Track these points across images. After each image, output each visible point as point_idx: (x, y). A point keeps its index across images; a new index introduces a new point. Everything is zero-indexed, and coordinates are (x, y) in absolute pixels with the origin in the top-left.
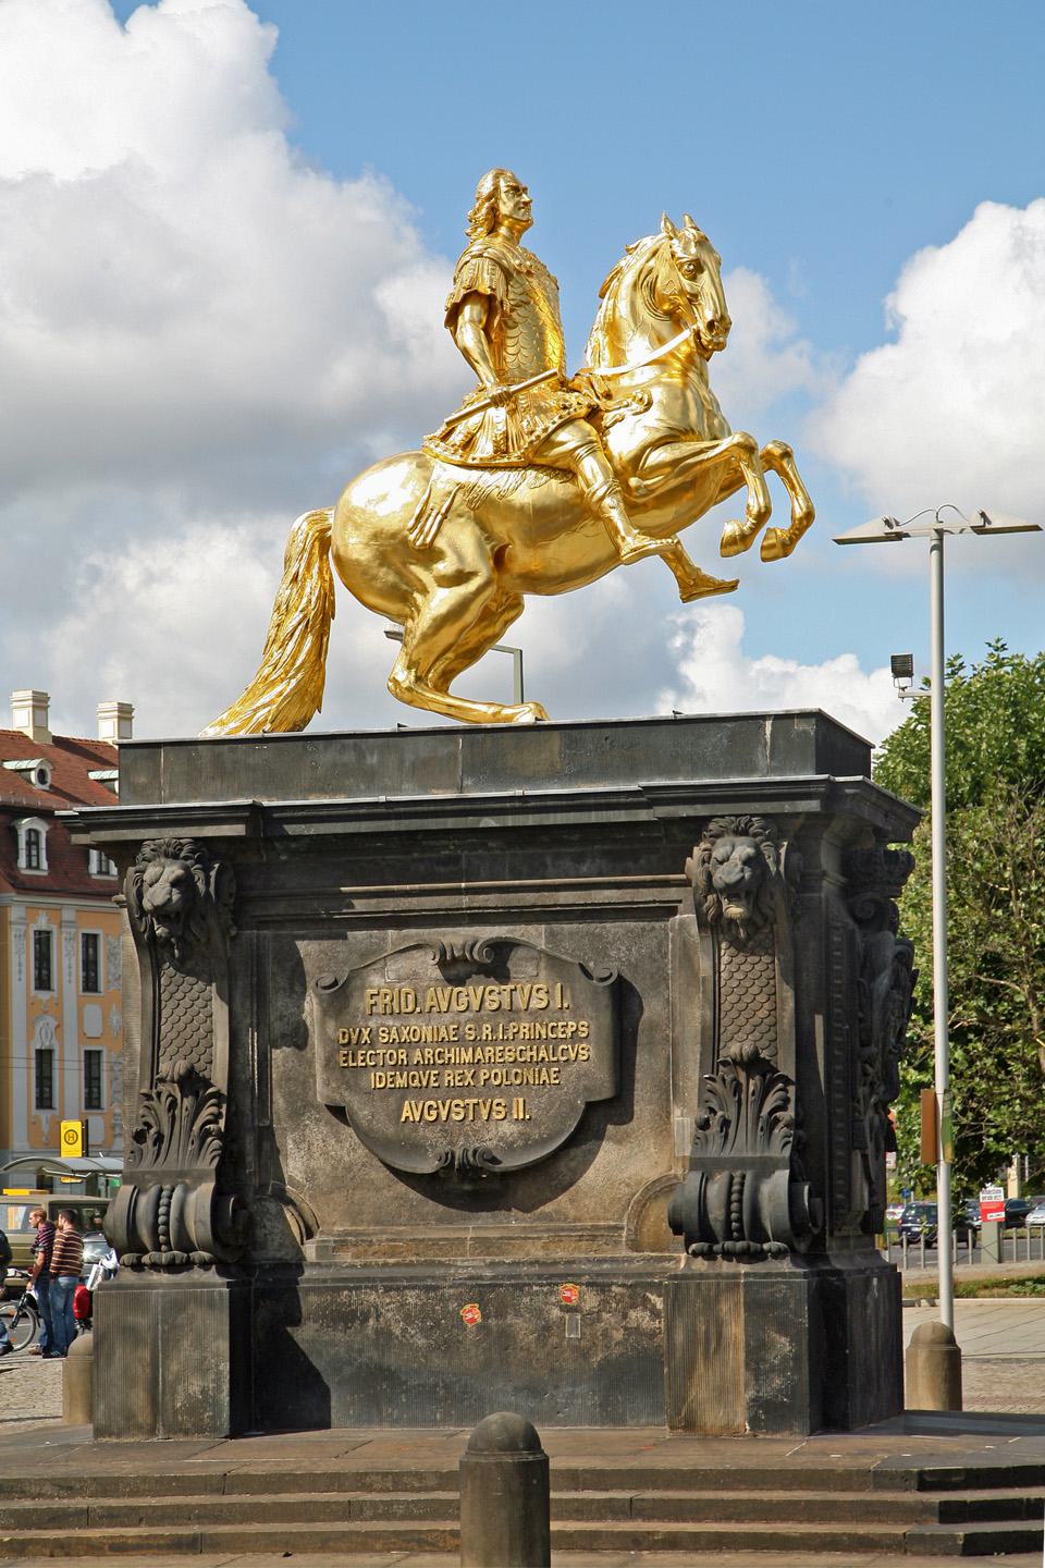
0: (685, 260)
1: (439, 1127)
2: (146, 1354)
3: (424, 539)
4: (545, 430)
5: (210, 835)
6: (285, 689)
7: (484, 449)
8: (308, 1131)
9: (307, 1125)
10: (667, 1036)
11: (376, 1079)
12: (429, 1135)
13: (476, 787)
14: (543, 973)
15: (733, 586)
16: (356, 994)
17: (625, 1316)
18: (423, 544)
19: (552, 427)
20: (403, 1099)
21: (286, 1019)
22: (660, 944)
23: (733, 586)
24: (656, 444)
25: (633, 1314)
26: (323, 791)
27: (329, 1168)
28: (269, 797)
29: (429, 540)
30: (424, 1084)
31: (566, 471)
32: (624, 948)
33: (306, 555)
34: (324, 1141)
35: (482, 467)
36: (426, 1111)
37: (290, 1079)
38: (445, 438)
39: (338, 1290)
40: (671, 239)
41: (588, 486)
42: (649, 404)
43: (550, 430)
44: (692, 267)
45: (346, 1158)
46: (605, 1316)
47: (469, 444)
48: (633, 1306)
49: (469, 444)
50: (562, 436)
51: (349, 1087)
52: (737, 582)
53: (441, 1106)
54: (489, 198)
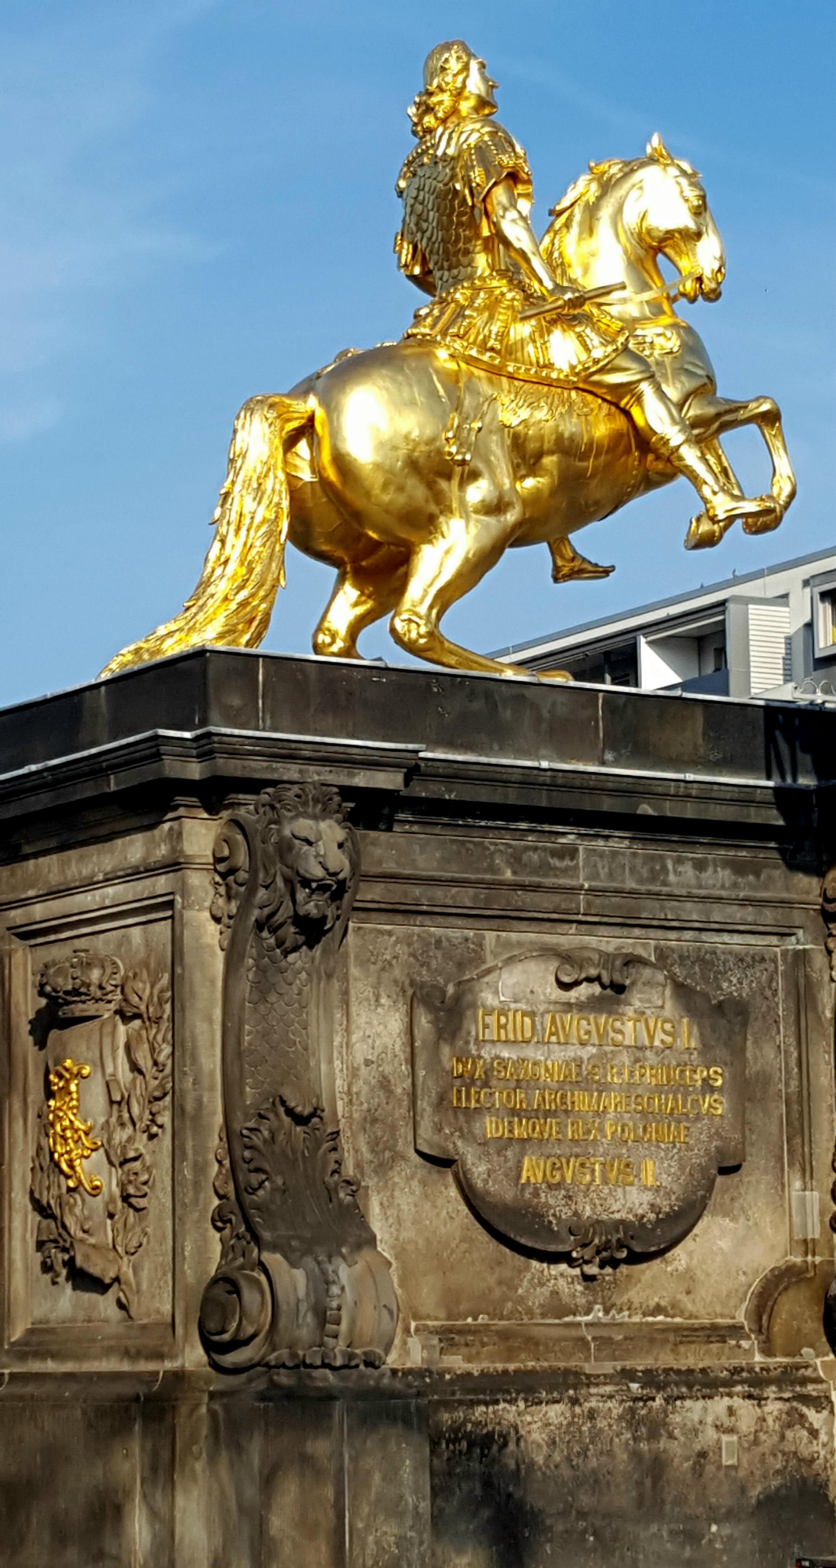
1: (563, 1192)
2: (329, 1492)
5: (362, 784)
8: (397, 1193)
9: (395, 1184)
10: (780, 1090)
11: (490, 1127)
12: (552, 1201)
13: (616, 763)
14: (669, 1005)
16: (469, 1013)
17: (783, 1437)
20: (523, 1154)
21: (370, 1041)
22: (771, 979)
25: (789, 1434)
26: (451, 745)
27: (421, 1242)
28: (434, 744)
30: (546, 1136)
32: (735, 980)
34: (416, 1206)
36: (548, 1173)
37: (375, 1120)
39: (473, 1404)
45: (443, 1230)
46: (763, 1437)
48: (790, 1425)
51: (462, 1136)
53: (565, 1165)
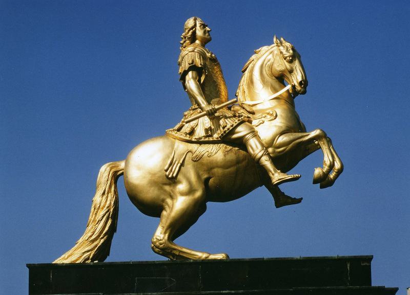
0: (288, 55)
3: (173, 174)
4: (232, 126)
6: (98, 244)
7: (200, 133)
15: (299, 201)
18: (172, 177)
19: (235, 125)
23: (299, 201)
24: (282, 133)
29: (174, 175)
31: (241, 144)
33: (109, 182)
35: (199, 142)
38: (179, 130)
40: (279, 46)
41: (253, 151)
42: (276, 116)
43: (234, 126)
44: (291, 58)
47: (192, 132)
49: (192, 132)
50: (239, 129)
52: (302, 199)
54: (192, 28)
